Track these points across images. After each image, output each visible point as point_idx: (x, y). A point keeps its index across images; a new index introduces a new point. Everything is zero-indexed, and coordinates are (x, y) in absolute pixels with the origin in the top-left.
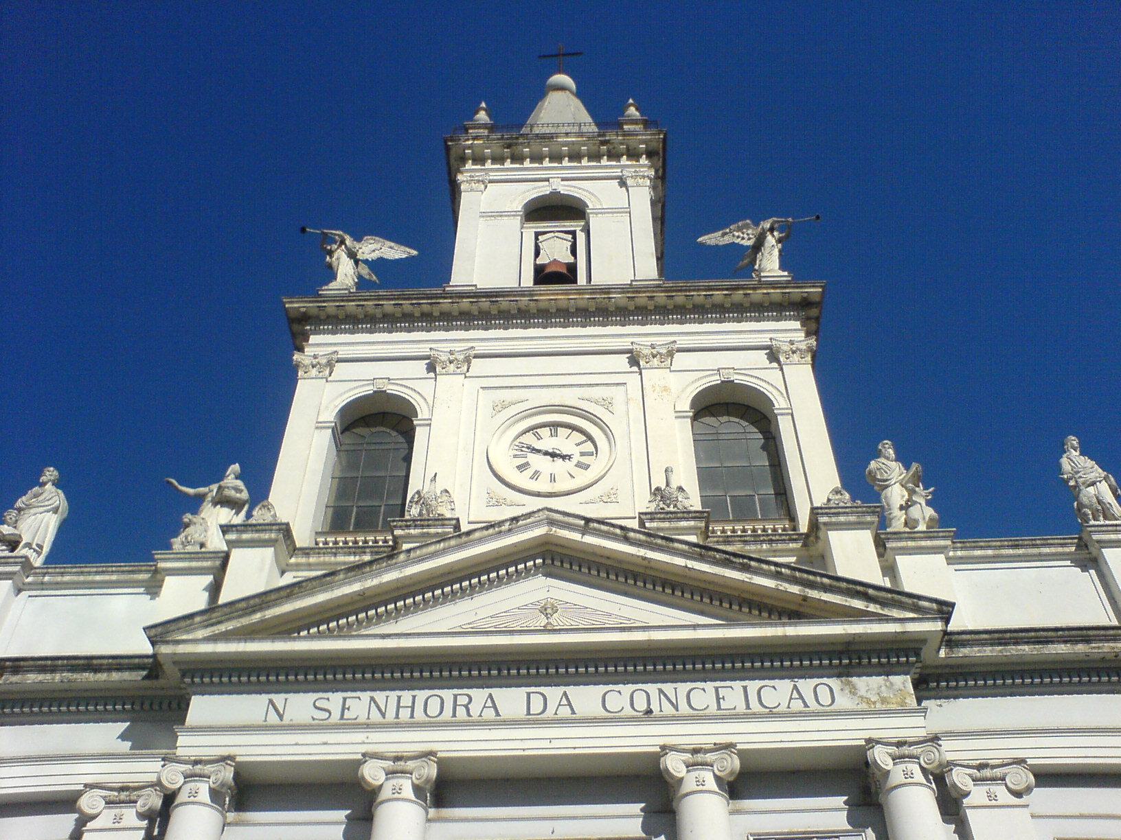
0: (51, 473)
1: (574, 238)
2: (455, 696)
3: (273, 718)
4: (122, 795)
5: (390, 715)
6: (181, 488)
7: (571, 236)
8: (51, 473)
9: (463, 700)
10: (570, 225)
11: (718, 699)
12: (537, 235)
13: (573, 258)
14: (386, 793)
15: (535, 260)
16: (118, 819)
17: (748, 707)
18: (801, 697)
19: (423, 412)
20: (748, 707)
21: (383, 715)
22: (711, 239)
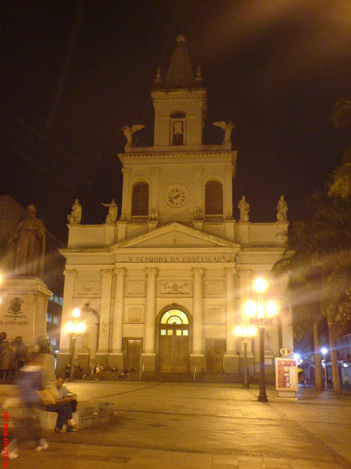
0: (77, 201)
1: (183, 124)
2: (159, 258)
3: (130, 261)
4: (108, 271)
5: (149, 261)
6: (104, 204)
7: (182, 124)
8: (77, 201)
9: (161, 258)
10: (182, 119)
11: (202, 259)
12: (174, 122)
13: (182, 132)
14: (149, 274)
15: (173, 132)
16: (107, 275)
17: (207, 261)
18: (216, 259)
19: (150, 185)
20: (207, 261)
21: (148, 260)
22: (216, 124)
